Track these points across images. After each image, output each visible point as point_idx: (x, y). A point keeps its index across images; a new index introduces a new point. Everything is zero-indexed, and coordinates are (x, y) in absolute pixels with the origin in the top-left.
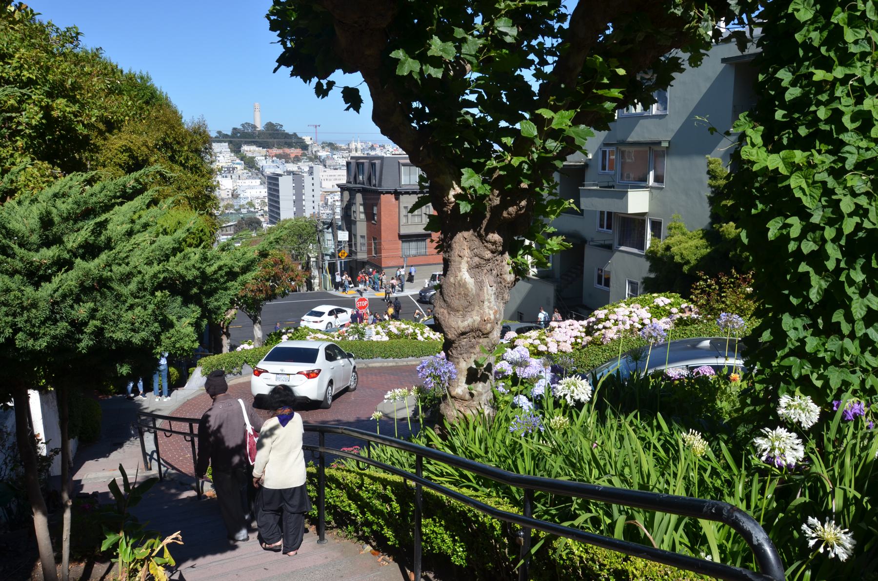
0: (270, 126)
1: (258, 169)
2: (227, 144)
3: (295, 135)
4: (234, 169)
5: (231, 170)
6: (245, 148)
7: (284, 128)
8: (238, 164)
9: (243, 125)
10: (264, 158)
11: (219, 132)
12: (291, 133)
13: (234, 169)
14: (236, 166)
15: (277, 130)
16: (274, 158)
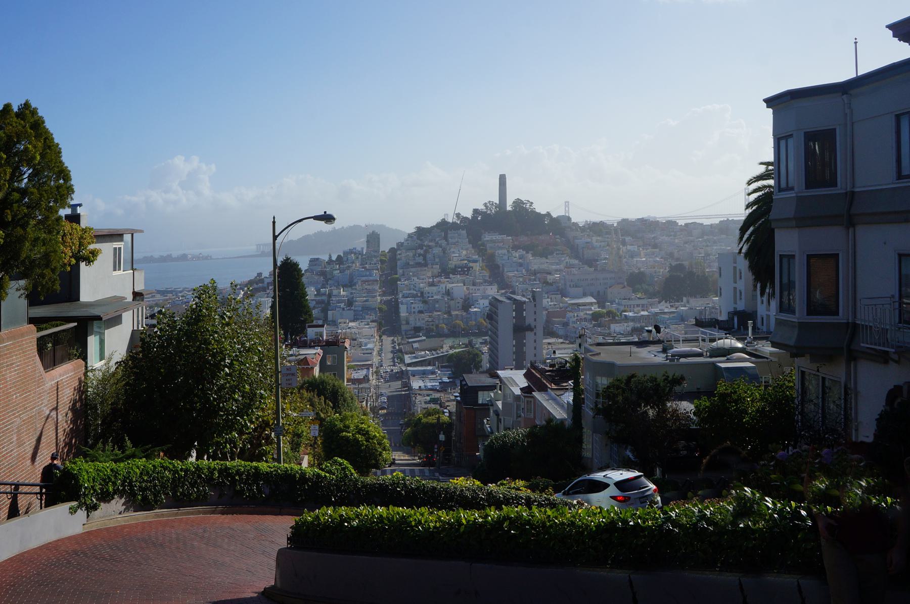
0: (518, 203)
1: (497, 267)
2: (464, 232)
3: (548, 214)
4: (469, 268)
5: (464, 270)
6: (487, 237)
7: (534, 206)
8: (475, 261)
9: (485, 205)
10: (505, 251)
11: (458, 215)
12: (544, 212)
13: (469, 268)
14: (471, 264)
15: (526, 210)
16: (521, 252)
